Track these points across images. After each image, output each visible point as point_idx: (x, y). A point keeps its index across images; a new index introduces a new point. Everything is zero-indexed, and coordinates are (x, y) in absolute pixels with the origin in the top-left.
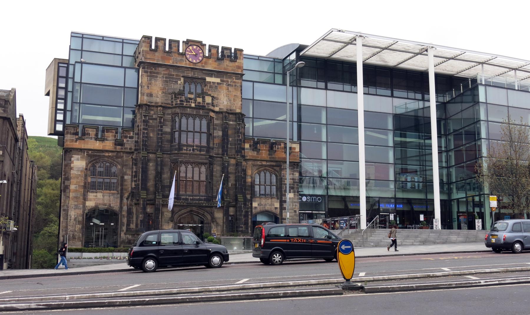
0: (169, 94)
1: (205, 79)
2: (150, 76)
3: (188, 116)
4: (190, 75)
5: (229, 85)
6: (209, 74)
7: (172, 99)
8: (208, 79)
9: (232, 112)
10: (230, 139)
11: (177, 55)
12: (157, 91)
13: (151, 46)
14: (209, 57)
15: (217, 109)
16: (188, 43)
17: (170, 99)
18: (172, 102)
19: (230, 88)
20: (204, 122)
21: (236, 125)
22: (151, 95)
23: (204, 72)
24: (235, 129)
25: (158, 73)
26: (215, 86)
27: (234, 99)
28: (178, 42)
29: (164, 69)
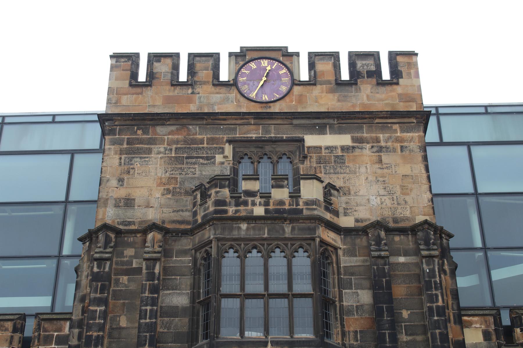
0: (187, 193)
1: (302, 140)
2: (128, 152)
3: (243, 247)
4: (254, 136)
5: (381, 149)
6: (314, 125)
7: (194, 205)
8: (311, 140)
9: (401, 225)
10: (405, 314)
11: (210, 88)
12: (150, 190)
13: (134, 75)
14: (312, 82)
15: (346, 222)
16: (243, 56)
17: (190, 207)
18: (195, 214)
19: (385, 158)
20: (302, 262)
21: (418, 265)
22: (128, 202)
23: (295, 122)
24: (418, 277)
25: (152, 141)
26: (339, 158)
27: (402, 187)
28: (215, 57)
29: (173, 128)
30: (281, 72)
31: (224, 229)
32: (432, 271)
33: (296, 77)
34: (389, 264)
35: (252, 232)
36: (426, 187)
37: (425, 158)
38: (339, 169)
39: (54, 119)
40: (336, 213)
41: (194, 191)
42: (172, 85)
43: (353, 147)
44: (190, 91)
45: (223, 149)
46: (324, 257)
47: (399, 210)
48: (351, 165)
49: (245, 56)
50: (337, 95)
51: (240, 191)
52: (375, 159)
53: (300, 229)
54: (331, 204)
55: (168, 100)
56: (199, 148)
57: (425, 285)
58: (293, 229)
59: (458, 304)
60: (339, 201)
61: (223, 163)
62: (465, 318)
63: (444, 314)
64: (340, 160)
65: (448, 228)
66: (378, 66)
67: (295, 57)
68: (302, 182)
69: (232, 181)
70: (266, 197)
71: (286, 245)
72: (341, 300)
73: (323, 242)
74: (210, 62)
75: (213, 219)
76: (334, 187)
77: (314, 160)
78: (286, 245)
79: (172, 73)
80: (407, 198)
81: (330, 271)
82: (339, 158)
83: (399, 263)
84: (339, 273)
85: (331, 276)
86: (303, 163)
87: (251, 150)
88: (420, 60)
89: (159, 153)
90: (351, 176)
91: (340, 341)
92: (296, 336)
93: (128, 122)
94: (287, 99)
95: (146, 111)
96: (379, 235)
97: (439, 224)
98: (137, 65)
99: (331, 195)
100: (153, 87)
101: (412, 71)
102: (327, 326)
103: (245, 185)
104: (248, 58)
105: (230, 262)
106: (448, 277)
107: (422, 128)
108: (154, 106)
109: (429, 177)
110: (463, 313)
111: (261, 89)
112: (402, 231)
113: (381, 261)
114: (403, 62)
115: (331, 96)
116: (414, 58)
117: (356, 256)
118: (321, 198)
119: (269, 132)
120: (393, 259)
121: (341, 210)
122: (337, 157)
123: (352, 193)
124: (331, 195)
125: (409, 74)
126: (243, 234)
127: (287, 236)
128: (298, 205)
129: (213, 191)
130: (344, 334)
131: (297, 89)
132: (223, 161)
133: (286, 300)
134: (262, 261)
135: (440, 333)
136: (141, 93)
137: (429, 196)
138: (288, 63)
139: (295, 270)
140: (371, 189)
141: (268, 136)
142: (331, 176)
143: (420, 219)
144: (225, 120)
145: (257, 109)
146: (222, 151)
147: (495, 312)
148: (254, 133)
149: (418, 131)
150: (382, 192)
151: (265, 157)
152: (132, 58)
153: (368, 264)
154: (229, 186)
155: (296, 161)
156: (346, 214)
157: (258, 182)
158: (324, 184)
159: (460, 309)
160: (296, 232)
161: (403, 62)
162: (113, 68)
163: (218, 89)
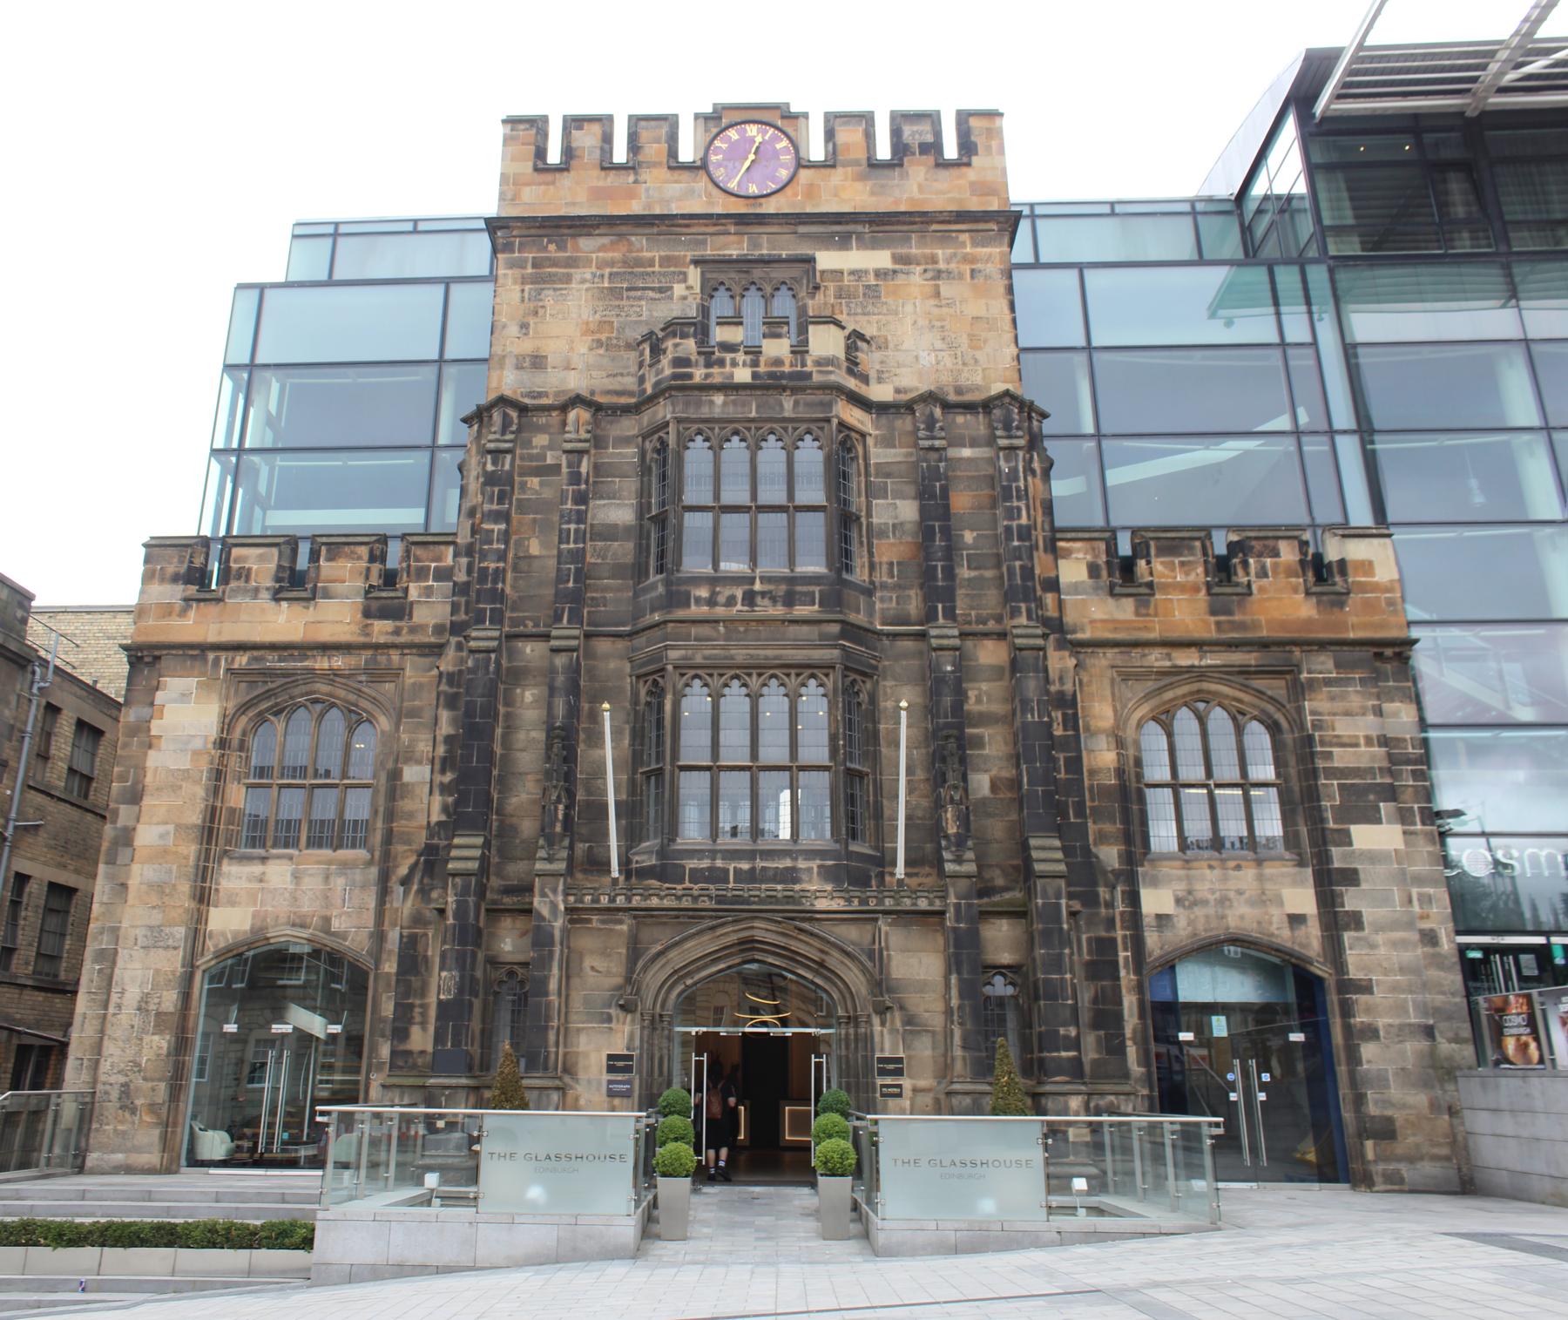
0: (629, 347)
1: (811, 260)
2: (537, 280)
3: (718, 432)
4: (734, 253)
5: (938, 275)
6: (833, 234)
7: (641, 365)
8: (827, 260)
9: (968, 398)
10: (969, 537)
11: (663, 173)
12: (571, 340)
13: (541, 153)
14: (829, 164)
15: (880, 392)
16: (717, 120)
17: (634, 368)
18: (642, 380)
19: (946, 289)
20: (811, 456)
21: (993, 461)
22: (537, 362)
23: (802, 229)
24: (991, 481)
25: (572, 263)
26: (872, 289)
27: (971, 337)
28: (671, 121)
29: (606, 240)
30: (778, 146)
31: (687, 404)
32: (1014, 470)
33: (802, 154)
34: (947, 460)
35: (731, 409)
36: (1009, 336)
37: (1010, 290)
38: (870, 308)
39: (415, 228)
40: (865, 379)
41: (639, 344)
42: (603, 169)
43: (895, 272)
44: (631, 178)
45: (685, 274)
46: (843, 451)
47: (965, 374)
48: (890, 301)
49: (720, 118)
50: (870, 183)
51: (712, 343)
52: (929, 291)
53: (807, 404)
54: (857, 364)
55: (597, 194)
56: (648, 274)
57: (1002, 492)
58: (796, 403)
59: (1052, 522)
60: (869, 359)
61: (685, 298)
62: (1061, 544)
63: (1029, 538)
64: (872, 293)
65: (1041, 403)
66: (938, 134)
67: (802, 120)
68: (811, 328)
69: (701, 329)
70: (755, 352)
71: (785, 429)
72: (869, 515)
73: (842, 425)
74: (664, 129)
75: (670, 388)
76: (862, 337)
77: (831, 292)
78: (785, 429)
79: (602, 149)
80: (978, 355)
81: (853, 470)
82: (872, 289)
83: (961, 459)
84: (867, 474)
85: (855, 479)
86: (813, 298)
87: (730, 276)
88: (1007, 125)
89: (583, 281)
90: (890, 318)
91: (866, 578)
92: (798, 569)
93: (533, 232)
94: (788, 191)
95: (562, 213)
96: (932, 414)
97: (1027, 397)
98: (546, 136)
99: (857, 349)
100: (572, 173)
101: (994, 143)
102: (847, 554)
103: (720, 334)
104: (725, 122)
105: (697, 457)
106: (1038, 481)
107: (1006, 240)
108: (574, 204)
109: (1014, 321)
110: (1059, 535)
111: (744, 176)
112: (969, 407)
113: (934, 455)
114: (978, 129)
115: (859, 185)
116: (997, 120)
117: (894, 447)
118: (842, 355)
119: (757, 246)
120: (953, 452)
121: (873, 375)
122: (868, 287)
123: (891, 345)
124: (857, 349)
125: (988, 149)
126: (717, 412)
127: (786, 414)
128: (804, 365)
129: (669, 344)
130: (872, 567)
131: (804, 174)
132: (685, 295)
133: (785, 515)
134: (747, 455)
135: (1022, 567)
136: (553, 183)
137: (1015, 351)
138: (789, 130)
139: (798, 468)
140: (922, 338)
141: (757, 253)
142: (859, 318)
143: (997, 388)
144: (687, 226)
145: (740, 208)
146: (684, 278)
147: (1109, 535)
148: (735, 247)
149: (1001, 245)
150: (939, 344)
151: (753, 288)
152: (538, 124)
153: (913, 459)
154: (695, 336)
155: (803, 294)
156: (880, 380)
157: (740, 328)
158: (847, 332)
159: (1054, 530)
160: (801, 409)
161: (978, 129)
162: (507, 140)
163: (676, 175)
